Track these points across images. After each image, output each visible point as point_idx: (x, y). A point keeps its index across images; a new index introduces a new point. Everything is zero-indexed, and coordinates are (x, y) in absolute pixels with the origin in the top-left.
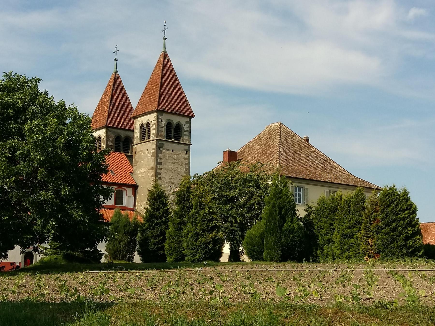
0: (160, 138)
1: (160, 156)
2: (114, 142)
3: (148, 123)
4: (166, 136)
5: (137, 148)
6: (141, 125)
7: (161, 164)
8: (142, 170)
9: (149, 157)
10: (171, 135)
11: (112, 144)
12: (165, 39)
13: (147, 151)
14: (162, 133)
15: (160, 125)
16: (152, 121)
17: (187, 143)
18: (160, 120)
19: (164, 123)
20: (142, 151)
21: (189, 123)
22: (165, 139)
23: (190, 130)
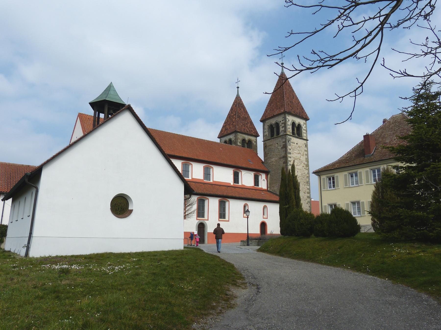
1: (289, 147)
2: (241, 143)
3: (277, 123)
4: (292, 132)
5: (267, 143)
6: (269, 126)
7: (290, 153)
8: (273, 159)
9: (280, 149)
10: (294, 132)
11: (240, 144)
13: (277, 145)
14: (289, 130)
16: (280, 122)
17: (305, 138)
18: (288, 120)
20: (272, 145)
21: (306, 124)
22: (292, 134)
23: (306, 129)
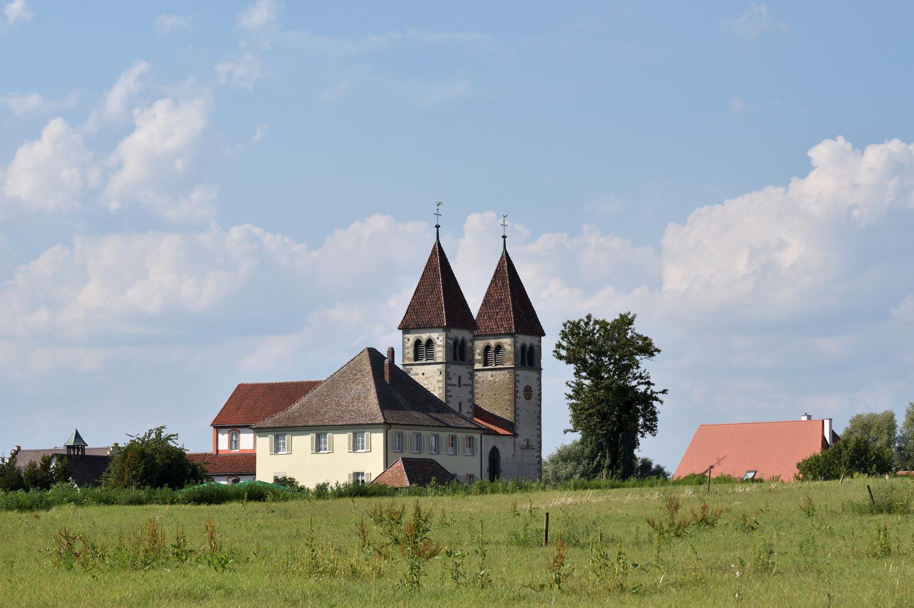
0: (407, 362)
11: (480, 357)
14: (409, 355)
15: (407, 345)
18: (406, 340)
19: (411, 343)
22: (413, 362)
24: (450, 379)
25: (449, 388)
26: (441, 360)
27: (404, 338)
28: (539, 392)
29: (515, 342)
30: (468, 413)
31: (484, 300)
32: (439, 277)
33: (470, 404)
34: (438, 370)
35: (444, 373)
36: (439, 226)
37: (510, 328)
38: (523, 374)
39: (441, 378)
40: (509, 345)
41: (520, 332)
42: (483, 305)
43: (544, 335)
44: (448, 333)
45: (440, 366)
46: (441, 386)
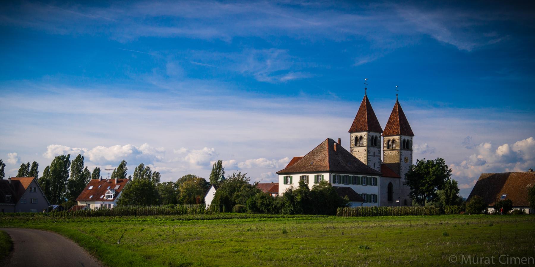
0: (352, 146)
11: (386, 145)
12: (366, 89)
15: (352, 139)
18: (352, 137)
19: (353, 138)
24: (370, 153)
25: (369, 157)
26: (366, 145)
27: (351, 136)
28: (411, 160)
29: (400, 138)
30: (378, 168)
31: (388, 121)
32: (365, 110)
33: (379, 164)
34: (364, 149)
35: (367, 151)
36: (366, 89)
37: (398, 132)
38: (404, 152)
39: (365, 153)
40: (398, 140)
41: (402, 134)
42: (387, 123)
43: (414, 136)
44: (369, 134)
45: (365, 148)
46: (366, 156)
